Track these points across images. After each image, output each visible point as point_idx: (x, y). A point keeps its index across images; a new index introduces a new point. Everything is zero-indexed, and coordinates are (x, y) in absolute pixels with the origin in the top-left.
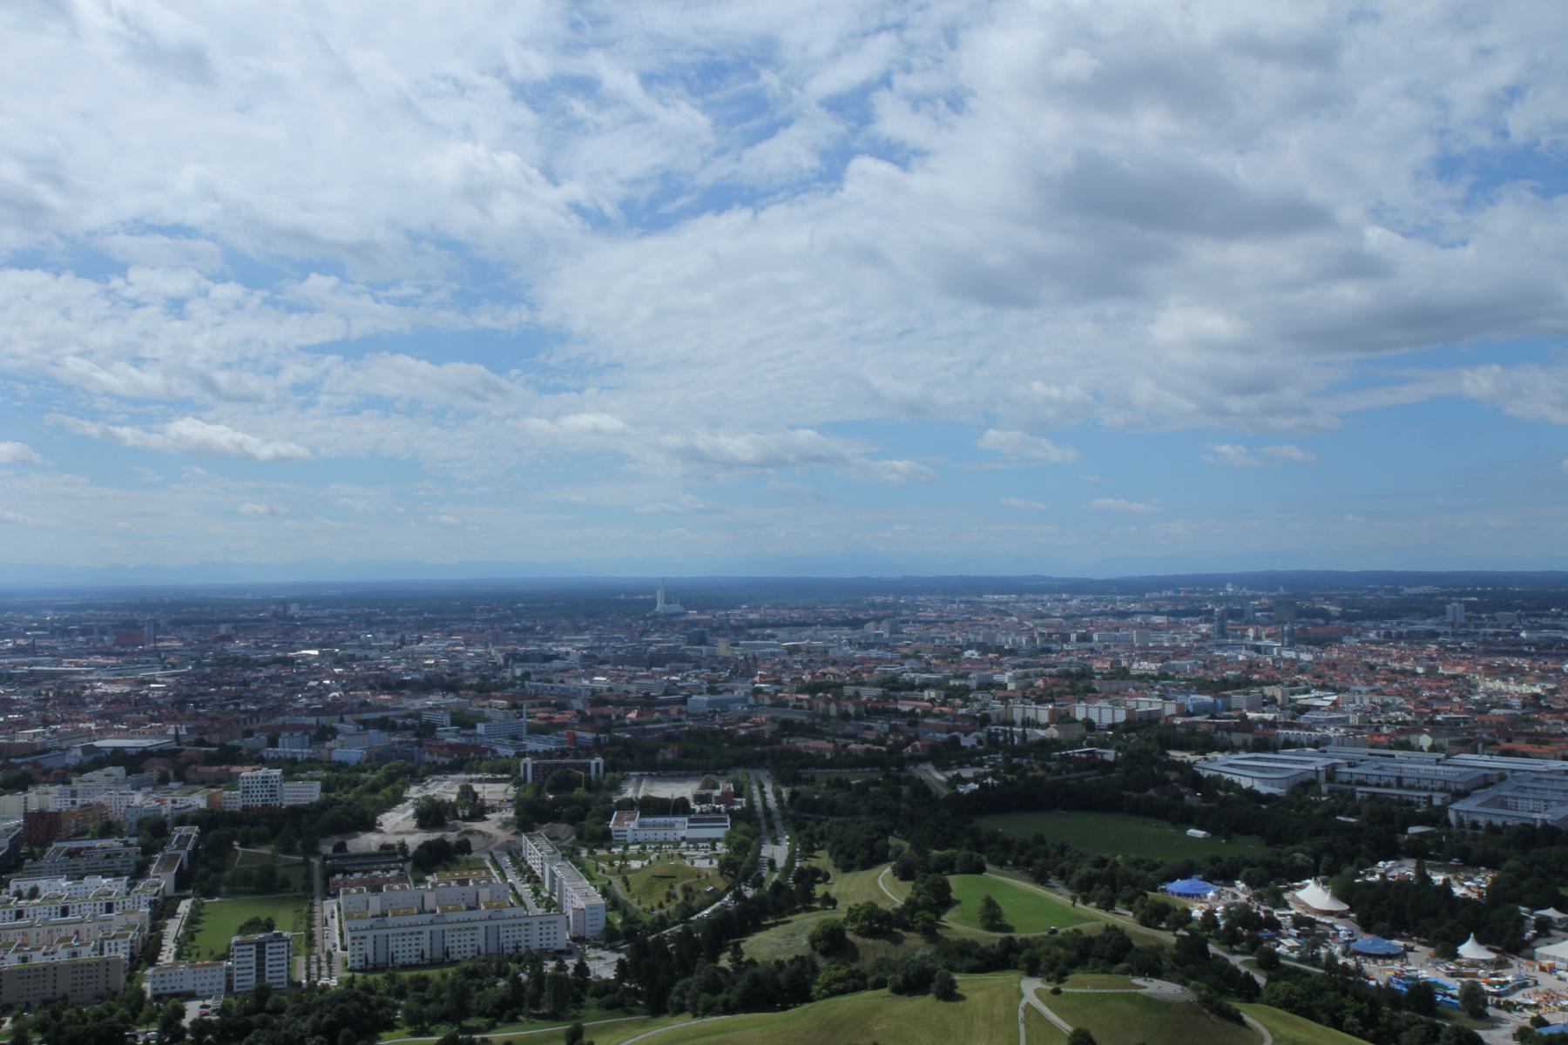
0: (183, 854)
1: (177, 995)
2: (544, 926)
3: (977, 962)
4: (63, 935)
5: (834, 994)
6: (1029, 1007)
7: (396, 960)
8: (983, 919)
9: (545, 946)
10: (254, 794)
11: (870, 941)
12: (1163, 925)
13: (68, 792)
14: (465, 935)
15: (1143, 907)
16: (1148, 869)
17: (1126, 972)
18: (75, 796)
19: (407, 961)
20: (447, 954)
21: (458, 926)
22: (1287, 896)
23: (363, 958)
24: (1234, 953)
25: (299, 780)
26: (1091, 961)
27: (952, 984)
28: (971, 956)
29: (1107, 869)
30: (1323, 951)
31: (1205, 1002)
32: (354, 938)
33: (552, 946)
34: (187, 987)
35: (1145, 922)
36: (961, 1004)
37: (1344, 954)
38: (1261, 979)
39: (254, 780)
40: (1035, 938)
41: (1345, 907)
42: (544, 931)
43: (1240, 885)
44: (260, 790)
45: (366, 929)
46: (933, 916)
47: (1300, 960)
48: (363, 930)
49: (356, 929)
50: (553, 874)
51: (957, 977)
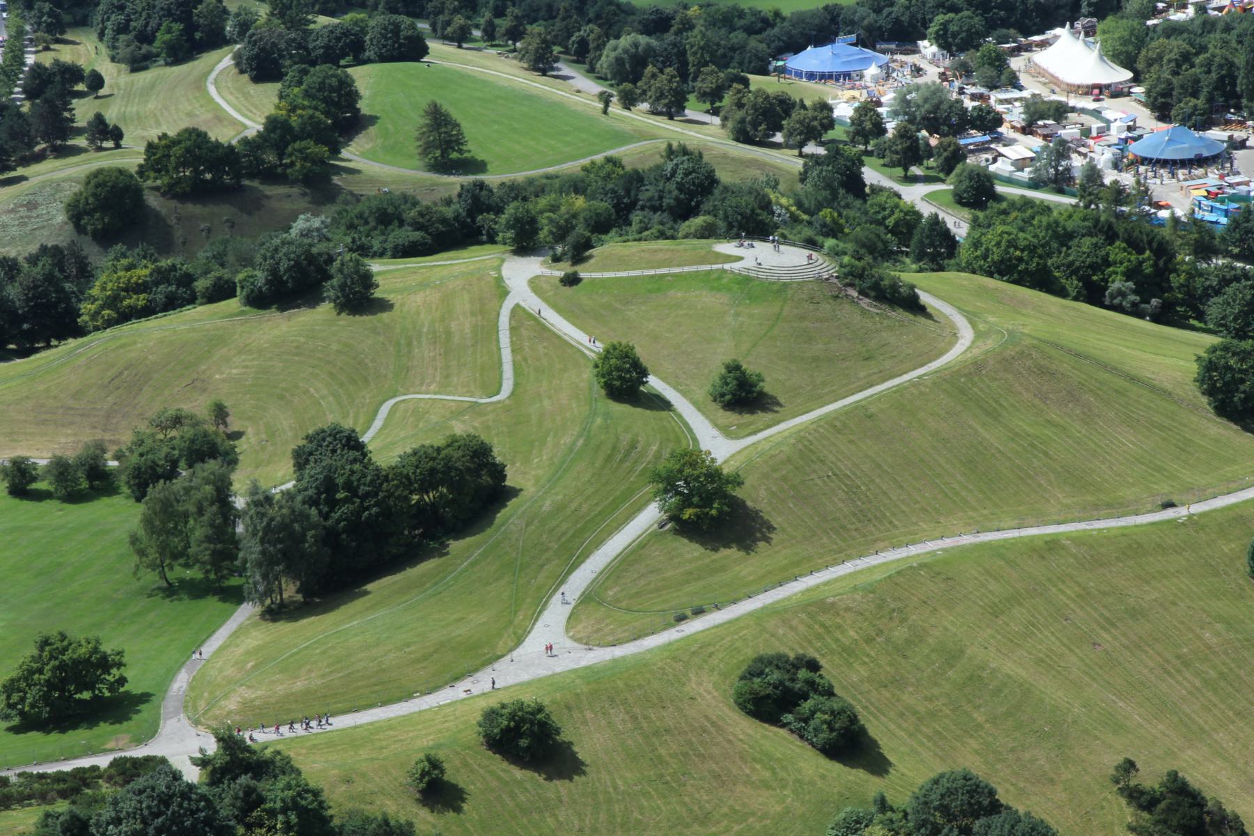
3: (417, 236)
5: (124, 317)
6: (518, 313)
8: (426, 150)
11: (192, 208)
12: (779, 138)
15: (740, 105)
16: (751, 31)
17: (708, 232)
22: (1015, 63)
24: (911, 180)
26: (636, 217)
27: (367, 280)
28: (401, 223)
29: (669, 37)
30: (1077, 162)
31: (853, 277)
35: (743, 136)
36: (385, 316)
37: (1116, 165)
38: (959, 225)
40: (531, 182)
41: (1129, 75)
43: (928, 48)
46: (324, 150)
47: (1035, 184)
51: (375, 266)
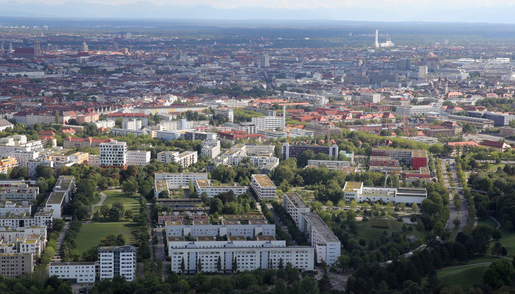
0: (66, 193)
2: (299, 255)
9: (299, 267)
10: (108, 157)
14: (247, 256)
19: (209, 270)
21: (243, 250)
32: (175, 253)
33: (304, 267)
34: (72, 276)
39: (108, 148)
42: (299, 258)
44: (112, 155)
45: (183, 248)
48: (180, 248)
49: (176, 248)
50: (306, 222)
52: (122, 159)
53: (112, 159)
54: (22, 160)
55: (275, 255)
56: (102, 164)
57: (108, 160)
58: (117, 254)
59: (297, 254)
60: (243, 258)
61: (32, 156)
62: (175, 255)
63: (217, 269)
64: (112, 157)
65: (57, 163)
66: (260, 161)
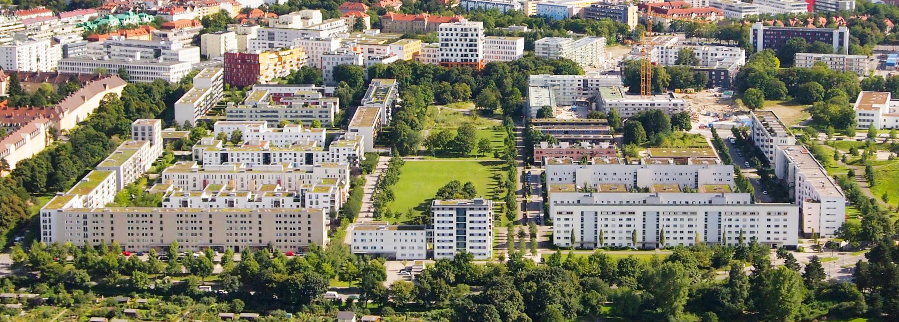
1: (377, 256)
4: (266, 182)
7: (605, 241)
9: (772, 240)
10: (453, 48)
13: (266, 34)
14: (682, 220)
18: (273, 39)
19: (617, 243)
20: (660, 238)
23: (569, 235)
25: (500, 34)
32: (560, 213)
33: (781, 240)
34: (388, 248)
39: (453, 32)
42: (772, 223)
44: (458, 42)
45: (574, 204)
48: (569, 204)
52: (476, 51)
53: (458, 50)
54: (313, 52)
55: (730, 217)
56: (442, 60)
57: (453, 52)
58: (461, 212)
59: (769, 217)
60: (675, 223)
61: (330, 45)
62: (560, 216)
63: (631, 241)
64: (460, 47)
65: (369, 57)
66: (712, 55)
